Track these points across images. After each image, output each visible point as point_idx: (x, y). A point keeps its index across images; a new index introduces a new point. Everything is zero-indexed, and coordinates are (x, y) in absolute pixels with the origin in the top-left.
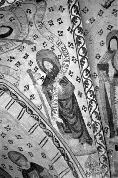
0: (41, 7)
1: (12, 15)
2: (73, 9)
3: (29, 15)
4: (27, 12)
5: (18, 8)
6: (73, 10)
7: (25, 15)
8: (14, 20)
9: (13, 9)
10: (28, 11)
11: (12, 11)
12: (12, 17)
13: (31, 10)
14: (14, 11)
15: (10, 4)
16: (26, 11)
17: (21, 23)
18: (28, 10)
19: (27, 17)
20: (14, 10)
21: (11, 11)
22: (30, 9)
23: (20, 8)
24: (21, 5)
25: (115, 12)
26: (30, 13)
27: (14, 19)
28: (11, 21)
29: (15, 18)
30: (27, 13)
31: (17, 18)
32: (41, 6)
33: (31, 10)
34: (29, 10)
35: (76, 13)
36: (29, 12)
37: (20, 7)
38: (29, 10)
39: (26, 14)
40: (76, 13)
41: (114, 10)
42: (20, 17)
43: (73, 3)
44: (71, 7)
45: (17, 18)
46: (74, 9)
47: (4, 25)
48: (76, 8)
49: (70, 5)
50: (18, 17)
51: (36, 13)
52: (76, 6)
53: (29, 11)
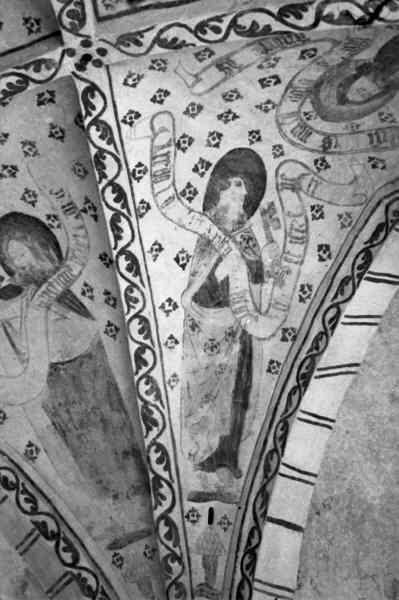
2: (17, 78)
6: (13, 79)
25: (10, 171)
35: (7, 89)
40: (7, 89)
41: (15, 168)
43: (35, 76)
44: (23, 71)
46: (18, 81)
48: (19, 88)
49: (26, 67)
52: (28, 85)
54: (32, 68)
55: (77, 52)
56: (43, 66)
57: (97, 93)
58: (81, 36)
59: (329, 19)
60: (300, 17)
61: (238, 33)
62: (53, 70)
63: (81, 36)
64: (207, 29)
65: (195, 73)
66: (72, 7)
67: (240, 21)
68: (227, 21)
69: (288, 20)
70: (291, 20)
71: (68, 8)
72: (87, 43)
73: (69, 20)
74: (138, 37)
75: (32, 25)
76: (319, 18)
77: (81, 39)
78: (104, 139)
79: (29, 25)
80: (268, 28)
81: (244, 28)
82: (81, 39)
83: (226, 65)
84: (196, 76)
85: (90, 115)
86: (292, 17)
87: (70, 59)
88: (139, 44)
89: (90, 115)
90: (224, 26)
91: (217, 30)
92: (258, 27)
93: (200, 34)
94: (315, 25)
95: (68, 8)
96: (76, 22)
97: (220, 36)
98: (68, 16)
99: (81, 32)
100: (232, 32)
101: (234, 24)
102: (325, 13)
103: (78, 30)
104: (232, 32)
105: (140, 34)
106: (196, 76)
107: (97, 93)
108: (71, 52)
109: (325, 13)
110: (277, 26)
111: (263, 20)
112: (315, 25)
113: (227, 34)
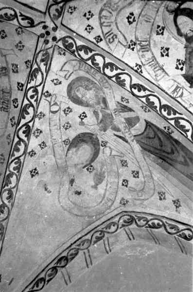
0: (111, 11)
1: (155, 37)
3: (136, 12)
4: (134, 20)
5: (139, 41)
7: (140, 17)
8: (160, 24)
9: (143, 46)
10: (131, 20)
11: (147, 45)
12: (158, 34)
13: (128, 18)
14: (146, 41)
15: (130, 76)
16: (134, 23)
17: (157, 10)
18: (130, 23)
19: (142, 10)
20: (144, 43)
21: (149, 45)
22: (127, 20)
23: (135, 38)
24: (131, 41)
26: (132, 14)
27: (159, 26)
28: (163, 28)
29: (157, 27)
30: (136, 19)
31: (153, 25)
32: (111, 13)
33: (128, 18)
34: (130, 20)
36: (133, 17)
37: (134, 40)
38: (129, 22)
39: (139, 18)
42: (150, 22)
43: (54, 7)
45: (153, 25)
47: (176, 34)
50: (151, 24)
51: (124, 8)
53: (131, 18)
54: (60, 10)
55: (53, 32)
56: (57, 14)
57: (29, 25)
58: (60, 40)
59: (19, 143)
60: (24, 132)
61: (27, 105)
62: (52, 16)
63: (60, 40)
64: (35, 93)
65: (7, 56)
66: (74, 48)
67: (31, 108)
68: (34, 104)
69: (24, 127)
70: (24, 129)
71: (75, 46)
72: (54, 39)
73: (70, 42)
74: (44, 63)
75: (72, 10)
76: (21, 140)
77: (58, 38)
78: (4, 14)
79: (73, 8)
80: (24, 118)
81: (28, 109)
82: (58, 38)
83: (4, 71)
84: (5, 56)
85: (20, 16)
86: (25, 129)
87: (52, 27)
88: (42, 60)
89: (20, 16)
90: (32, 101)
91: (32, 97)
92: (26, 114)
93: (32, 89)
94: (18, 137)
95: (75, 46)
96: (67, 44)
97: (29, 98)
98: (71, 43)
99: (61, 41)
100: (28, 103)
101: (32, 106)
102: (21, 143)
103: (63, 41)
104: (28, 103)
105: (46, 65)
106: (5, 56)
107: (29, 25)
108: (55, 29)
109: (21, 143)
110: (23, 122)
111: (28, 118)
112: (18, 137)
113: (28, 100)
